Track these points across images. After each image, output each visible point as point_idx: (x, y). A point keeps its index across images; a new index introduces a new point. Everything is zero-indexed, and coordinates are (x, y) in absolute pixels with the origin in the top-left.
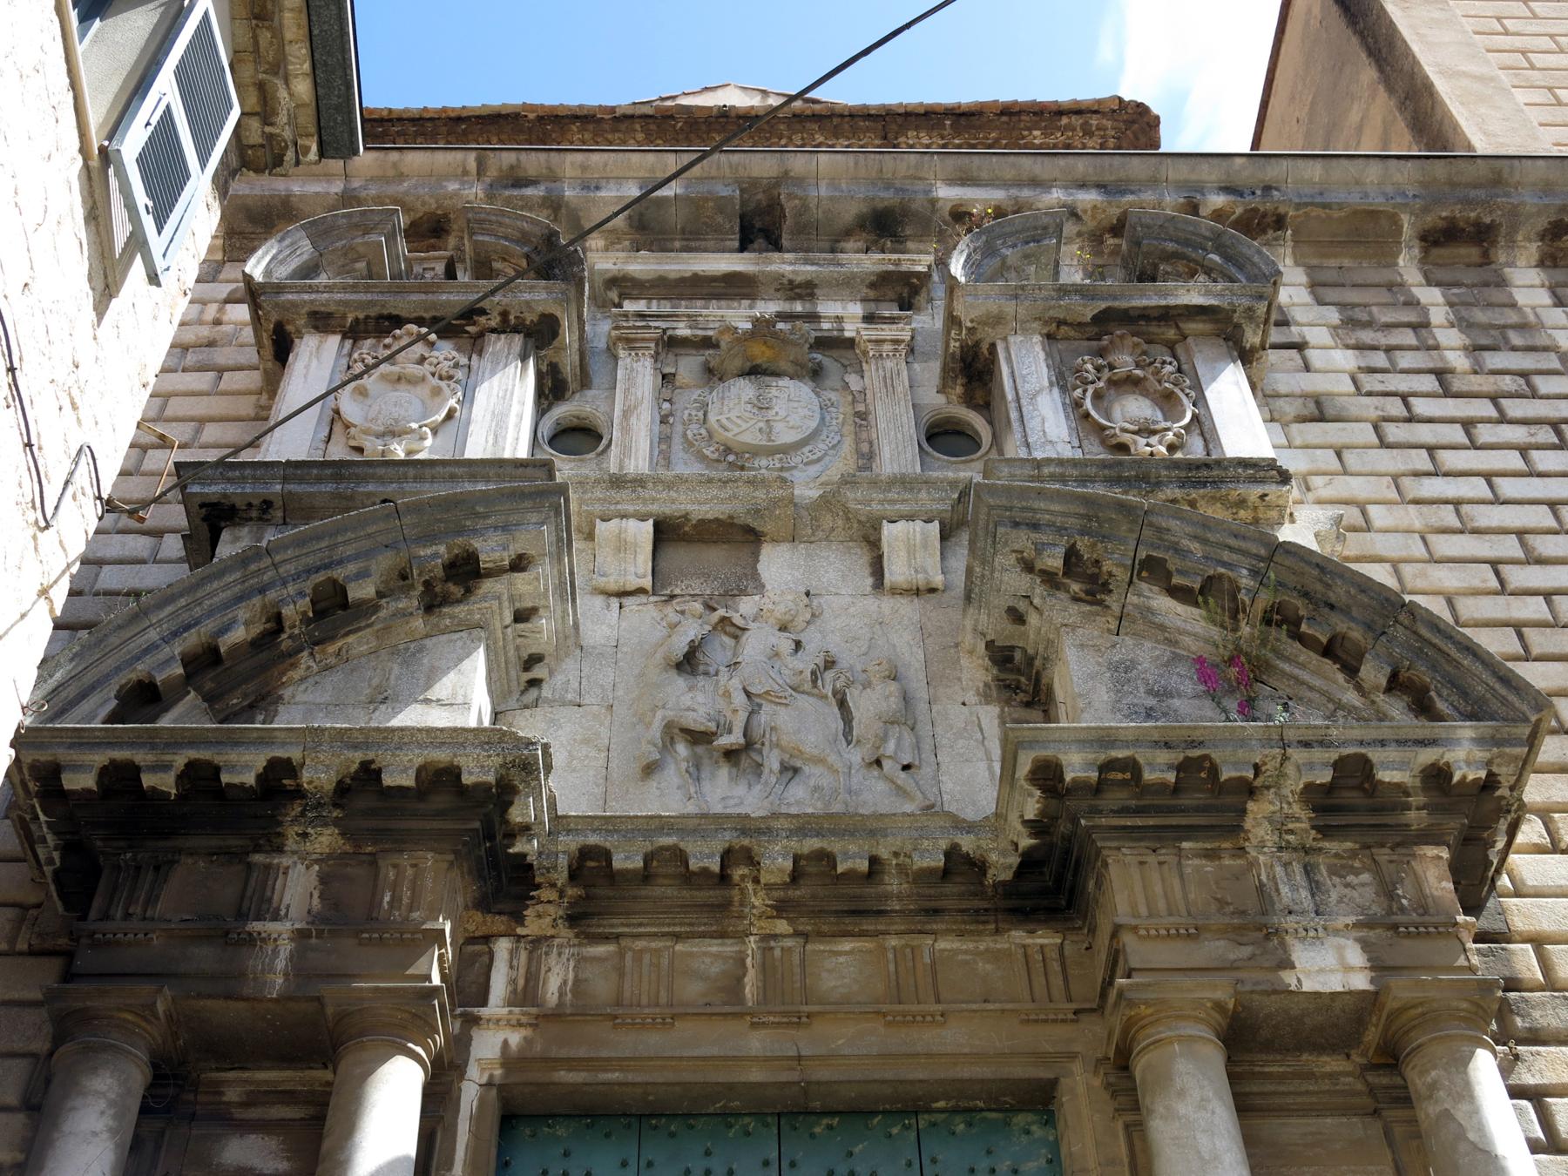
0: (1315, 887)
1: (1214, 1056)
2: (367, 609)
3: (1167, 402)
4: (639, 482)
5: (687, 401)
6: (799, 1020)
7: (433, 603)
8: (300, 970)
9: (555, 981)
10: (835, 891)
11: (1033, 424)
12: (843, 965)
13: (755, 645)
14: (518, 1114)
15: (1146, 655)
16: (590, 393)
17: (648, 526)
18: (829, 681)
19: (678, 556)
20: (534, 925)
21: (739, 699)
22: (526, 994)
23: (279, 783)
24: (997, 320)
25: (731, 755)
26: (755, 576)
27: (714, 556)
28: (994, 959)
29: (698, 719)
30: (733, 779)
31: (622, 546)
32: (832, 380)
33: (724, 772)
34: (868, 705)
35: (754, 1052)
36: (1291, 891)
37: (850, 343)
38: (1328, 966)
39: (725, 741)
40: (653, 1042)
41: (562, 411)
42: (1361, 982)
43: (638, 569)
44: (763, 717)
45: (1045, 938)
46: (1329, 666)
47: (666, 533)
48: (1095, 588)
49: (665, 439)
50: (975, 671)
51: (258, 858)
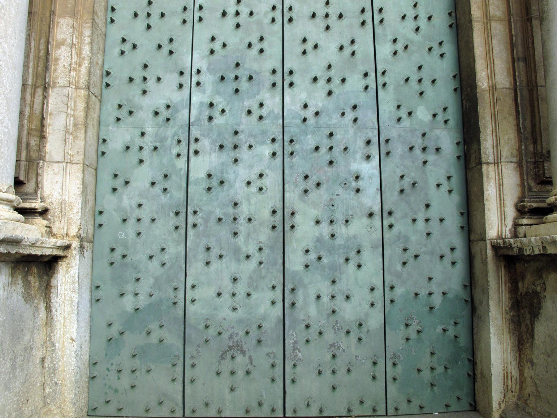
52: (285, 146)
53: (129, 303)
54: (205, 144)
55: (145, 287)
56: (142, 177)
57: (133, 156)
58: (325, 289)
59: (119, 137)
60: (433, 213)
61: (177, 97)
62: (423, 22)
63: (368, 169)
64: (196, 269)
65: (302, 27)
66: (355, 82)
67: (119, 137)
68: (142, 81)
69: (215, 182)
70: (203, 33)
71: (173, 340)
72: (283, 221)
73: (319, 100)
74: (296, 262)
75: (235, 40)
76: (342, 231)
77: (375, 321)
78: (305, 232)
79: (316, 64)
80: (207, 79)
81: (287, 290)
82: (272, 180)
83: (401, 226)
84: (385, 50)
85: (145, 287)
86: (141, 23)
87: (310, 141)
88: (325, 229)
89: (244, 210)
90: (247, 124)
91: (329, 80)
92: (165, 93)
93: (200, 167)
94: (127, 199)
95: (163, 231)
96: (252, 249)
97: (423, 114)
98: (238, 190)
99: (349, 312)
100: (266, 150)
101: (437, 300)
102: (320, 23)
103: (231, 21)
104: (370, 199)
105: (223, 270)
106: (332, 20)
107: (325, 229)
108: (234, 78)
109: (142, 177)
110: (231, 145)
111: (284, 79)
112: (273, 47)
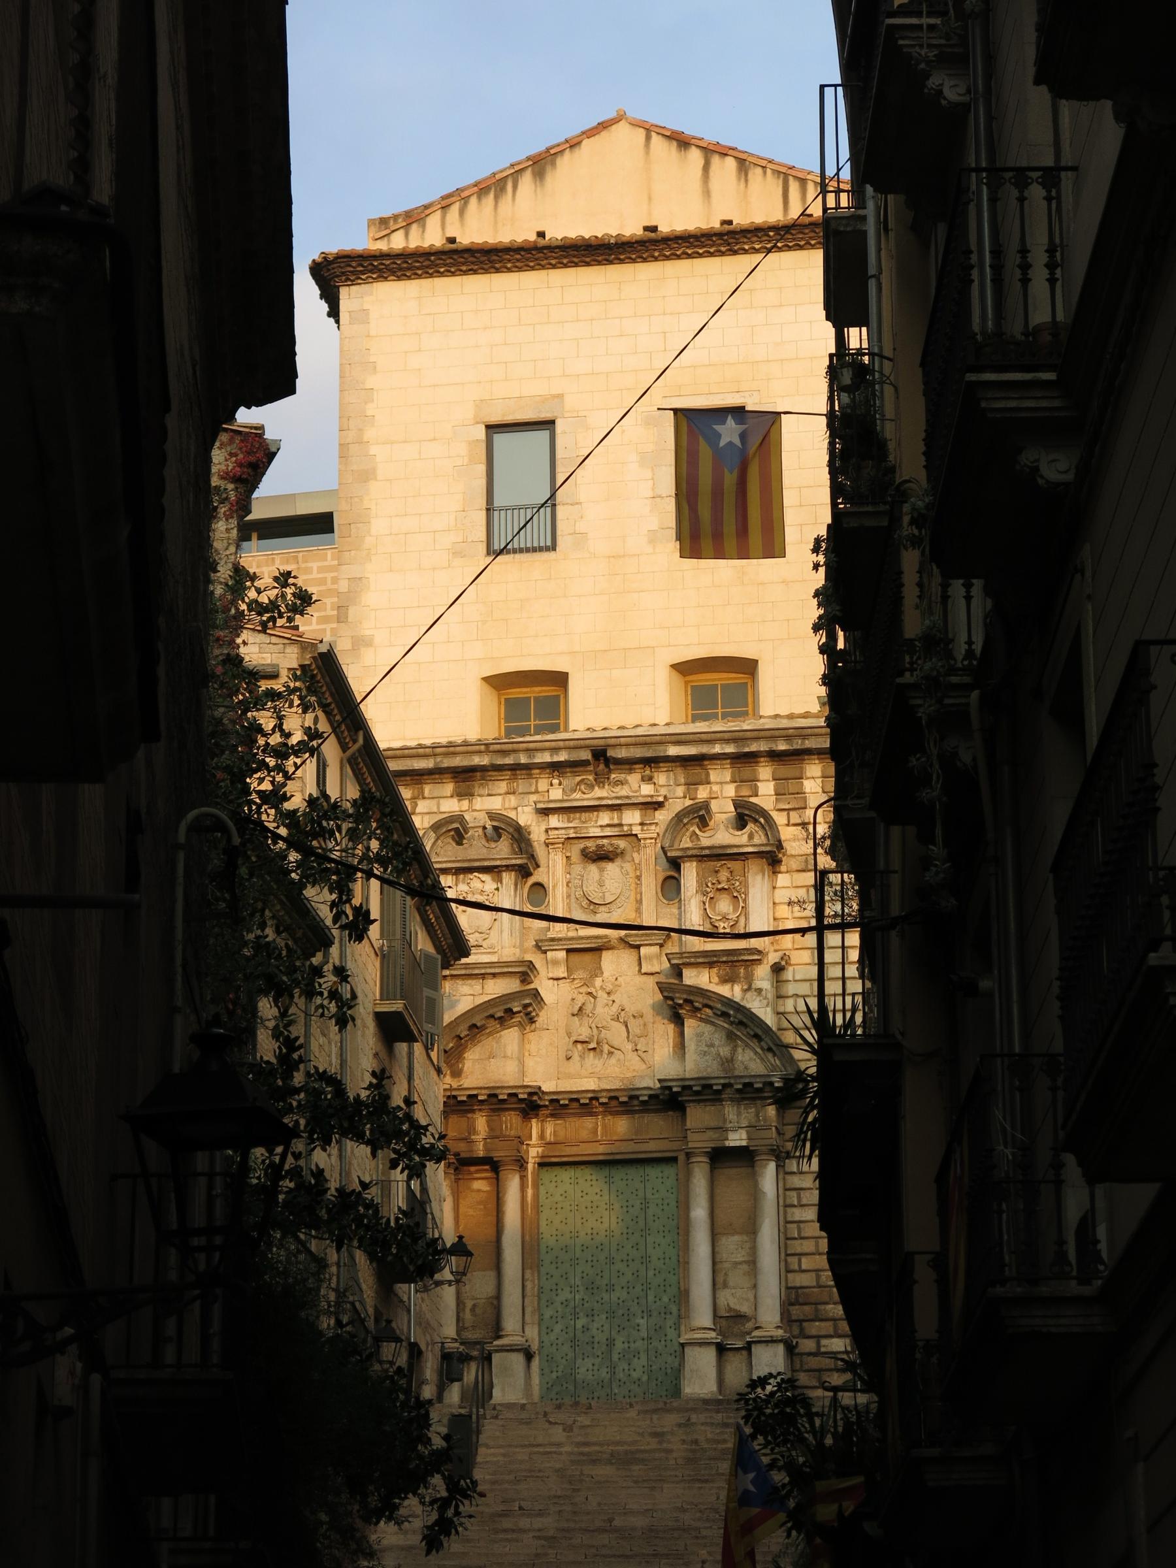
0: (739, 1114)
2: (483, 1027)
4: (560, 939)
8: (486, 1149)
9: (549, 1136)
11: (688, 915)
13: (602, 995)
14: (544, 1165)
15: (707, 1029)
16: (540, 869)
17: (563, 954)
19: (575, 957)
21: (595, 1029)
22: (542, 1136)
24: (680, 857)
25: (594, 1049)
26: (600, 968)
27: (587, 957)
29: (581, 1038)
30: (595, 1057)
31: (555, 963)
32: (628, 857)
33: (592, 1054)
34: (634, 1026)
37: (636, 835)
38: (737, 1139)
39: (592, 1046)
42: (744, 1143)
43: (561, 972)
44: (602, 1035)
46: (755, 1040)
47: (569, 951)
49: (569, 896)
51: (469, 1115)
52: (611, 1315)
53: (554, 1375)
54: (581, 1314)
55: (561, 1368)
56: (558, 1328)
57: (554, 1320)
58: (626, 1368)
59: (548, 1313)
60: (669, 1338)
61: (570, 1296)
62: (667, 1260)
63: (642, 1322)
64: (579, 1361)
66: (639, 1288)
67: (548, 1313)
69: (585, 1329)
71: (571, 1388)
72: (611, 1343)
73: (624, 1295)
74: (615, 1357)
76: (632, 1345)
77: (645, 1378)
78: (619, 1346)
80: (581, 1288)
81: (613, 1368)
83: (655, 1343)
84: (651, 1273)
85: (561, 1368)
86: (554, 1266)
87: (621, 1312)
88: (626, 1345)
89: (596, 1339)
92: (565, 1295)
93: (579, 1324)
94: (553, 1337)
95: (566, 1348)
96: (599, 1353)
97: (665, 1299)
99: (635, 1375)
100: (604, 1316)
101: (669, 1371)
102: (625, 1263)
103: (590, 1264)
104: (644, 1334)
105: (588, 1363)
106: (630, 1262)
107: (626, 1345)
108: (591, 1288)
109: (558, 1328)
110: (591, 1315)
111: (611, 1288)
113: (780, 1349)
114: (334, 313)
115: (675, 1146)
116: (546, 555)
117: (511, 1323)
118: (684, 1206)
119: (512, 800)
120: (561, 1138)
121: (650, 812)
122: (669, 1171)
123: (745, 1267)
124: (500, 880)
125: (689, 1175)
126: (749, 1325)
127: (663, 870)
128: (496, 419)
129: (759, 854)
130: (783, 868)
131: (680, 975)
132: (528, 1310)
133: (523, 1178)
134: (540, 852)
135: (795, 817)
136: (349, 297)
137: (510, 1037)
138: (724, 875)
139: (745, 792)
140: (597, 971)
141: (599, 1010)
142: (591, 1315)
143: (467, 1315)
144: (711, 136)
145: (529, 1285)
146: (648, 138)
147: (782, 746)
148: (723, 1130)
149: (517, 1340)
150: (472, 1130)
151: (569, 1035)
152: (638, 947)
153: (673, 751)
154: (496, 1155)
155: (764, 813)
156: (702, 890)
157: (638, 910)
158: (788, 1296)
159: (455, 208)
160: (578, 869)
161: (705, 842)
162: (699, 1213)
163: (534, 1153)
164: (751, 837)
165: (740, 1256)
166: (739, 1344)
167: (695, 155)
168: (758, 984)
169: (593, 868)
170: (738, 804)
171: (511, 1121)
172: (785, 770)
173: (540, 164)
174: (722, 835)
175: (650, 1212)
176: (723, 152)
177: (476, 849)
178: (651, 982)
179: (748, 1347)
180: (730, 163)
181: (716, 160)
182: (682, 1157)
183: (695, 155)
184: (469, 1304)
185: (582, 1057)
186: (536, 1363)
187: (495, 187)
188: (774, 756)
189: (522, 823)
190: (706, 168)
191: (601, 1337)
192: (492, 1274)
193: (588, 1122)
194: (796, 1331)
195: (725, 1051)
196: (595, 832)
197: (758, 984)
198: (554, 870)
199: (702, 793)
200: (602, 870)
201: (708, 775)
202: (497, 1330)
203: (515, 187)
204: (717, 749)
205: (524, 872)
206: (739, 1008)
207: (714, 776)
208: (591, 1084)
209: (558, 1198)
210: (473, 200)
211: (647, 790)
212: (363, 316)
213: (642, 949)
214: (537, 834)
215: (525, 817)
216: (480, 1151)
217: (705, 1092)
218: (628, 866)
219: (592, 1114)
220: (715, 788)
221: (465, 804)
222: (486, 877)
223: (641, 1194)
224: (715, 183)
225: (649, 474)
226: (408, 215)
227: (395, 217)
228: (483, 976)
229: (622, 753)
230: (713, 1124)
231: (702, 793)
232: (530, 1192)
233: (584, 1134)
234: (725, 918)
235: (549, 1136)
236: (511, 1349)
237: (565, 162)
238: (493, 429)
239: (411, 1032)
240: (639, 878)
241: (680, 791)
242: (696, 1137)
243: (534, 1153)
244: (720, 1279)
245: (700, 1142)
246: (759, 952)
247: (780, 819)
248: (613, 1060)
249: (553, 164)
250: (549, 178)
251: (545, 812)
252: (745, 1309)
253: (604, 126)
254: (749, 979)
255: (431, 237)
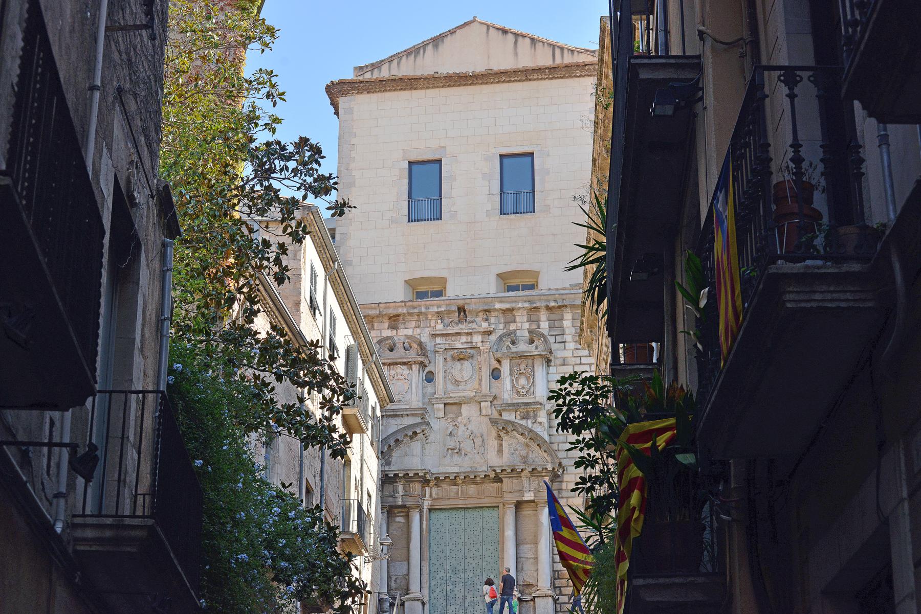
1: (513, 510)
3: (528, 379)
5: (450, 364)
6: (466, 499)
7: (411, 438)
9: (434, 495)
10: (469, 479)
12: (472, 489)
13: (462, 428)
14: (430, 510)
15: (514, 441)
18: (472, 436)
19: (448, 407)
20: (431, 484)
22: (431, 496)
23: (396, 475)
27: (454, 408)
28: (491, 488)
31: (439, 410)
32: (475, 358)
34: (478, 441)
35: (460, 503)
36: (526, 485)
38: (529, 496)
40: (447, 502)
41: (427, 370)
43: (441, 414)
45: (499, 484)
47: (445, 404)
48: (507, 433)
50: (494, 434)
52: (465, 584)
56: (438, 590)
59: (433, 583)
64: (448, 607)
65: (469, 560)
66: (479, 571)
68: (437, 572)
70: (449, 562)
72: (464, 598)
74: (467, 605)
75: (454, 562)
78: (468, 600)
79: (471, 567)
82: (462, 591)
84: (485, 564)
90: (458, 580)
91: (473, 571)
92: (441, 574)
93: (449, 588)
94: (435, 594)
98: (456, 592)
105: (453, 608)
108: (455, 571)
109: (438, 590)
110: (454, 584)
111: (465, 571)
112: (462, 564)
113: (550, 599)
114: (337, 113)
115: (497, 500)
116: (436, 222)
117: (414, 587)
118: (502, 530)
119: (418, 331)
120: (441, 495)
121: (486, 336)
122: (494, 512)
123: (532, 560)
124: (411, 368)
125: (504, 514)
126: (534, 589)
127: (494, 364)
128: (413, 159)
129: (541, 356)
130: (552, 364)
131: (501, 415)
132: (424, 581)
133: (421, 516)
134: (430, 355)
135: (559, 339)
136: (343, 102)
137: (416, 446)
138: (523, 367)
139: (534, 326)
140: (459, 414)
141: (460, 433)
142: (454, 584)
143: (393, 584)
144: (517, 30)
145: (424, 568)
146: (488, 29)
147: (552, 304)
148: (521, 492)
149: (418, 595)
150: (395, 491)
151: (445, 445)
152: (480, 403)
153: (498, 306)
154: (408, 504)
155: (543, 335)
156: (511, 374)
157: (480, 384)
158: (554, 574)
159: (395, 62)
160: (450, 364)
161: (514, 349)
162: (510, 533)
163: (427, 504)
164: (537, 348)
165: (530, 555)
166: (529, 598)
167: (510, 37)
168: (539, 420)
169: (458, 363)
170: (530, 331)
171: (416, 487)
172: (553, 316)
173: (437, 41)
174: (522, 347)
175: (485, 533)
176: (524, 36)
177: (399, 353)
178: (486, 420)
179: (534, 599)
180: (528, 41)
181: (520, 39)
182: (501, 506)
183: (510, 37)
184: (393, 578)
185: (452, 457)
186: (427, 607)
187: (415, 51)
188: (548, 308)
189: (423, 340)
190: (516, 42)
191: (460, 595)
192: (406, 563)
193: (454, 488)
194: (558, 592)
195: (524, 453)
196: (459, 345)
197: (539, 420)
198: (438, 366)
199: (512, 327)
200: (462, 365)
201: (514, 317)
202: (407, 591)
203: (424, 52)
204: (520, 305)
205: (422, 365)
206: (531, 431)
207: (518, 319)
208: (456, 469)
209: (438, 526)
210: (404, 58)
211: (485, 325)
212: (350, 111)
213: (483, 404)
214: (429, 346)
215: (425, 338)
216: (400, 503)
217: (515, 473)
218: (475, 363)
219: (455, 484)
220: (519, 325)
221: (395, 332)
222: (405, 367)
223: (480, 524)
224: (519, 50)
225: (487, 183)
226: (372, 65)
227: (367, 66)
228: (402, 416)
229: (473, 307)
230: (517, 488)
231: (512, 327)
232: (425, 523)
233: (452, 494)
234: (523, 388)
235: (434, 495)
236: (414, 600)
237: (448, 40)
238: (411, 163)
239: (362, 428)
240: (480, 368)
241: (501, 326)
242: (509, 495)
243: (427, 504)
244: (520, 567)
245: (512, 498)
246: (541, 404)
247: (552, 339)
248: (467, 458)
249: (443, 41)
250: (440, 48)
251: (435, 336)
252: (531, 581)
253: (466, 24)
254: (535, 417)
255: (384, 73)
